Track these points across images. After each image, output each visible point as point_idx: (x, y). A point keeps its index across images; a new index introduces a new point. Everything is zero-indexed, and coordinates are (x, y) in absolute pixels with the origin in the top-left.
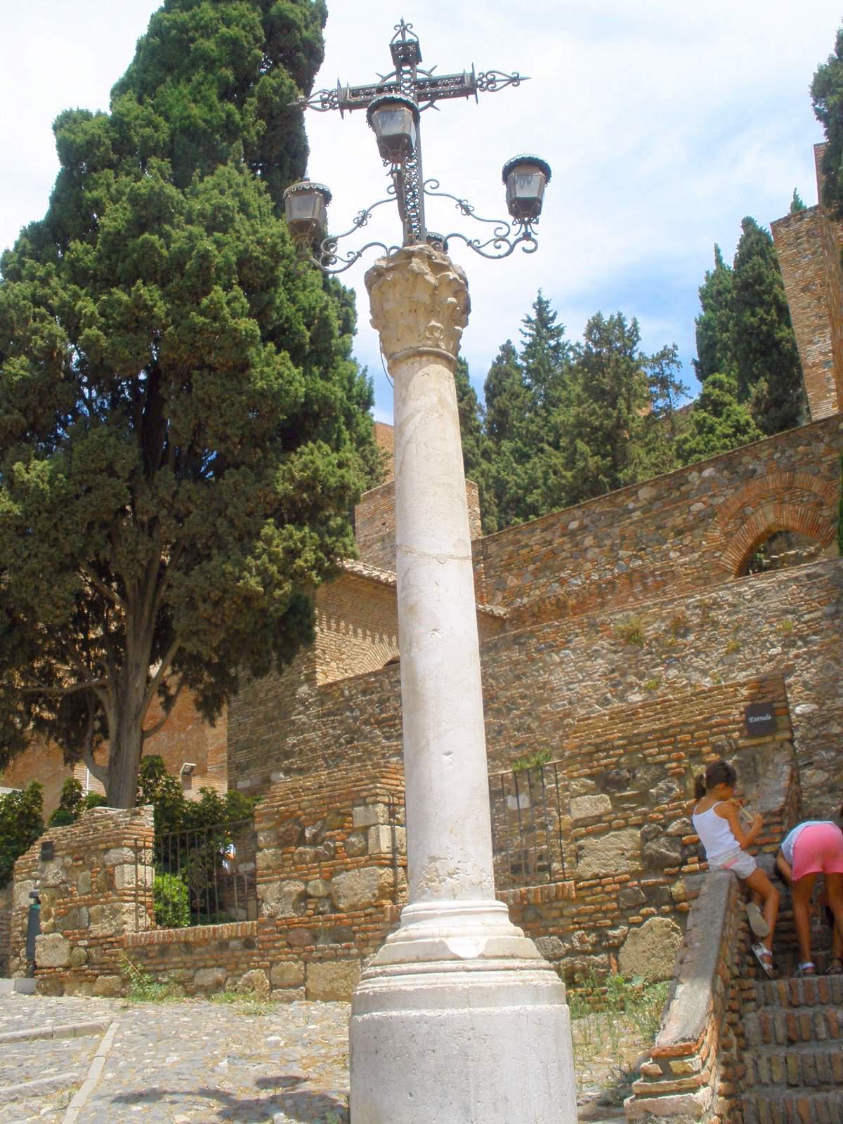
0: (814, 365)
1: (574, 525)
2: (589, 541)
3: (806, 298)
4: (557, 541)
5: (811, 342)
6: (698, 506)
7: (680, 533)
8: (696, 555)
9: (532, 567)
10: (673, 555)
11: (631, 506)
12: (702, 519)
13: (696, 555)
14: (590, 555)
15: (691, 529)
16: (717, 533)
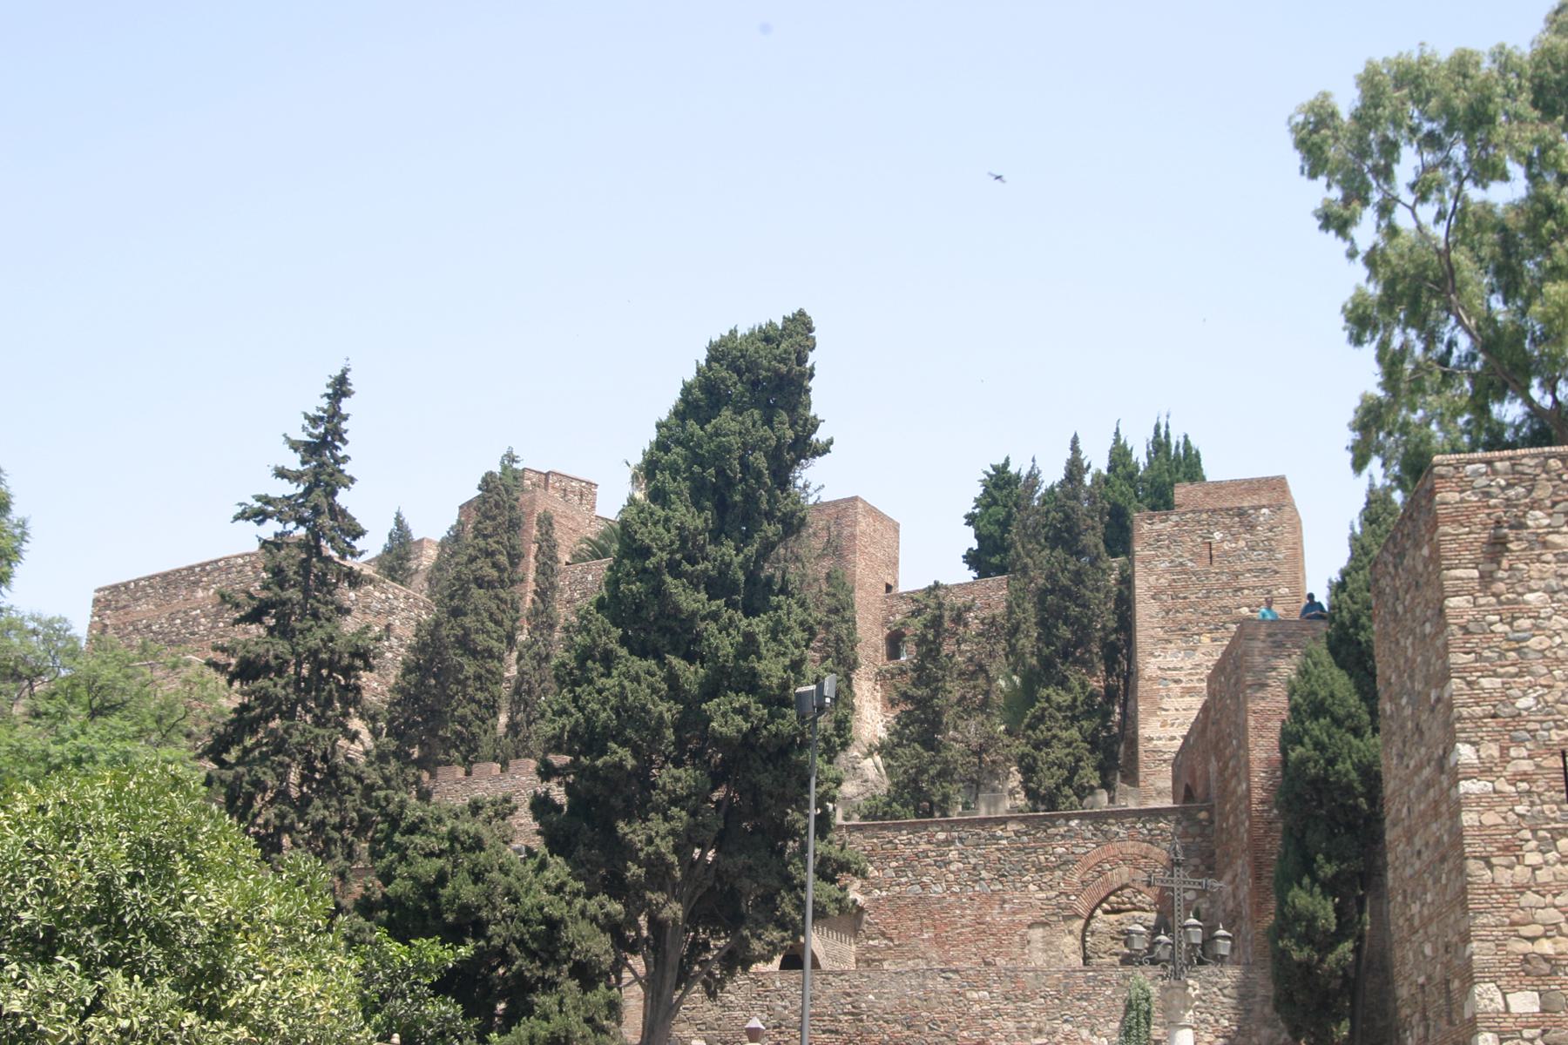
0: (1150, 679)
1: (941, 836)
2: (953, 855)
3: (1155, 607)
4: (923, 847)
5: (1152, 654)
6: (1060, 850)
7: (1039, 870)
8: (1053, 894)
9: (894, 864)
10: (1032, 887)
11: (999, 833)
12: (1064, 863)
13: (1053, 894)
14: (953, 868)
15: (1052, 870)
16: (1075, 879)
